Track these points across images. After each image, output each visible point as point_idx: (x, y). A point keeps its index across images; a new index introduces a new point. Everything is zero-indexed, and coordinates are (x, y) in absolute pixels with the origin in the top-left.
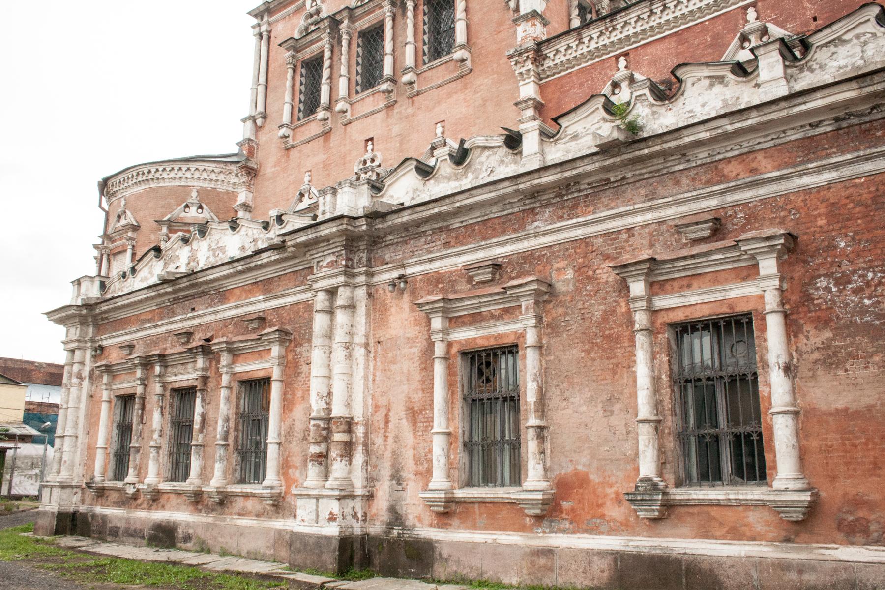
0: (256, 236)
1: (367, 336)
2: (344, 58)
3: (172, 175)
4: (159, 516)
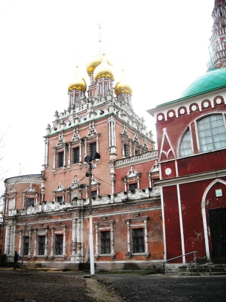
0: (58, 206)
1: (83, 228)
2: (69, 155)
3: (25, 180)
4: (37, 262)
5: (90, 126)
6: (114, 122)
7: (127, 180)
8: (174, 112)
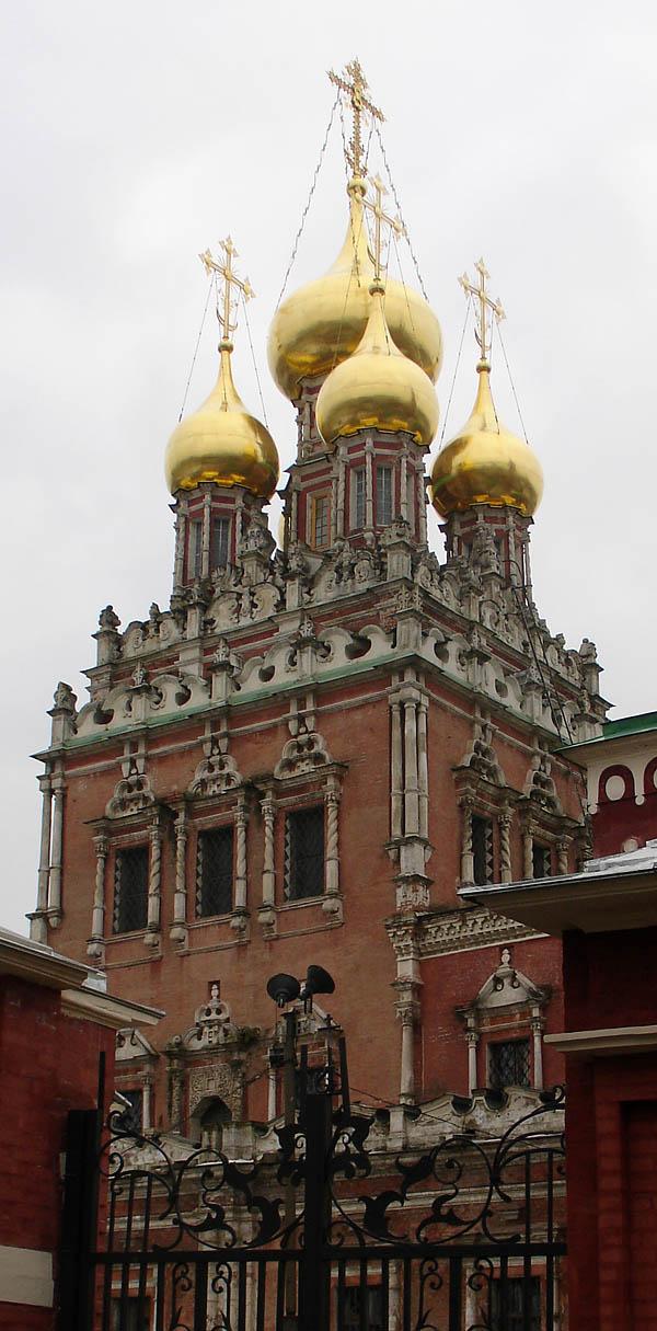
5: (294, 717)
6: (419, 705)
7: (478, 1020)
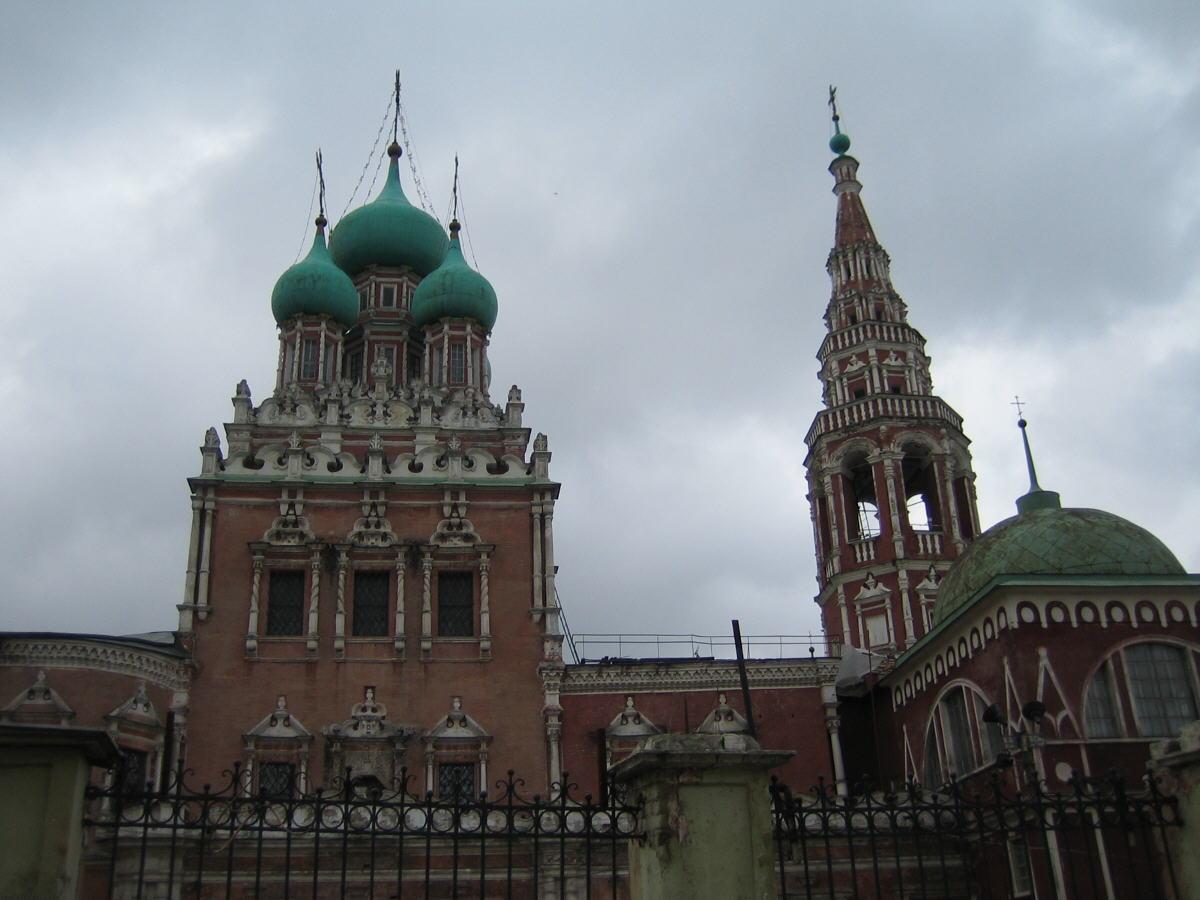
5: (449, 505)
8: (1066, 612)
